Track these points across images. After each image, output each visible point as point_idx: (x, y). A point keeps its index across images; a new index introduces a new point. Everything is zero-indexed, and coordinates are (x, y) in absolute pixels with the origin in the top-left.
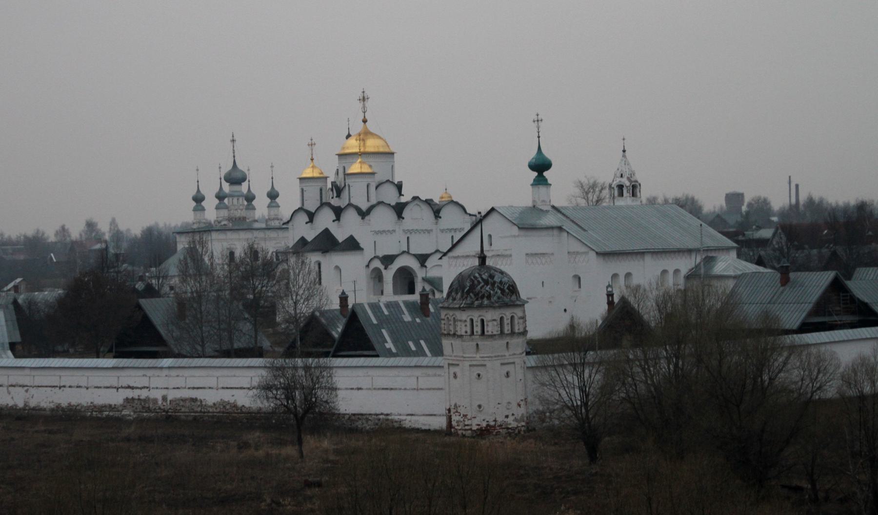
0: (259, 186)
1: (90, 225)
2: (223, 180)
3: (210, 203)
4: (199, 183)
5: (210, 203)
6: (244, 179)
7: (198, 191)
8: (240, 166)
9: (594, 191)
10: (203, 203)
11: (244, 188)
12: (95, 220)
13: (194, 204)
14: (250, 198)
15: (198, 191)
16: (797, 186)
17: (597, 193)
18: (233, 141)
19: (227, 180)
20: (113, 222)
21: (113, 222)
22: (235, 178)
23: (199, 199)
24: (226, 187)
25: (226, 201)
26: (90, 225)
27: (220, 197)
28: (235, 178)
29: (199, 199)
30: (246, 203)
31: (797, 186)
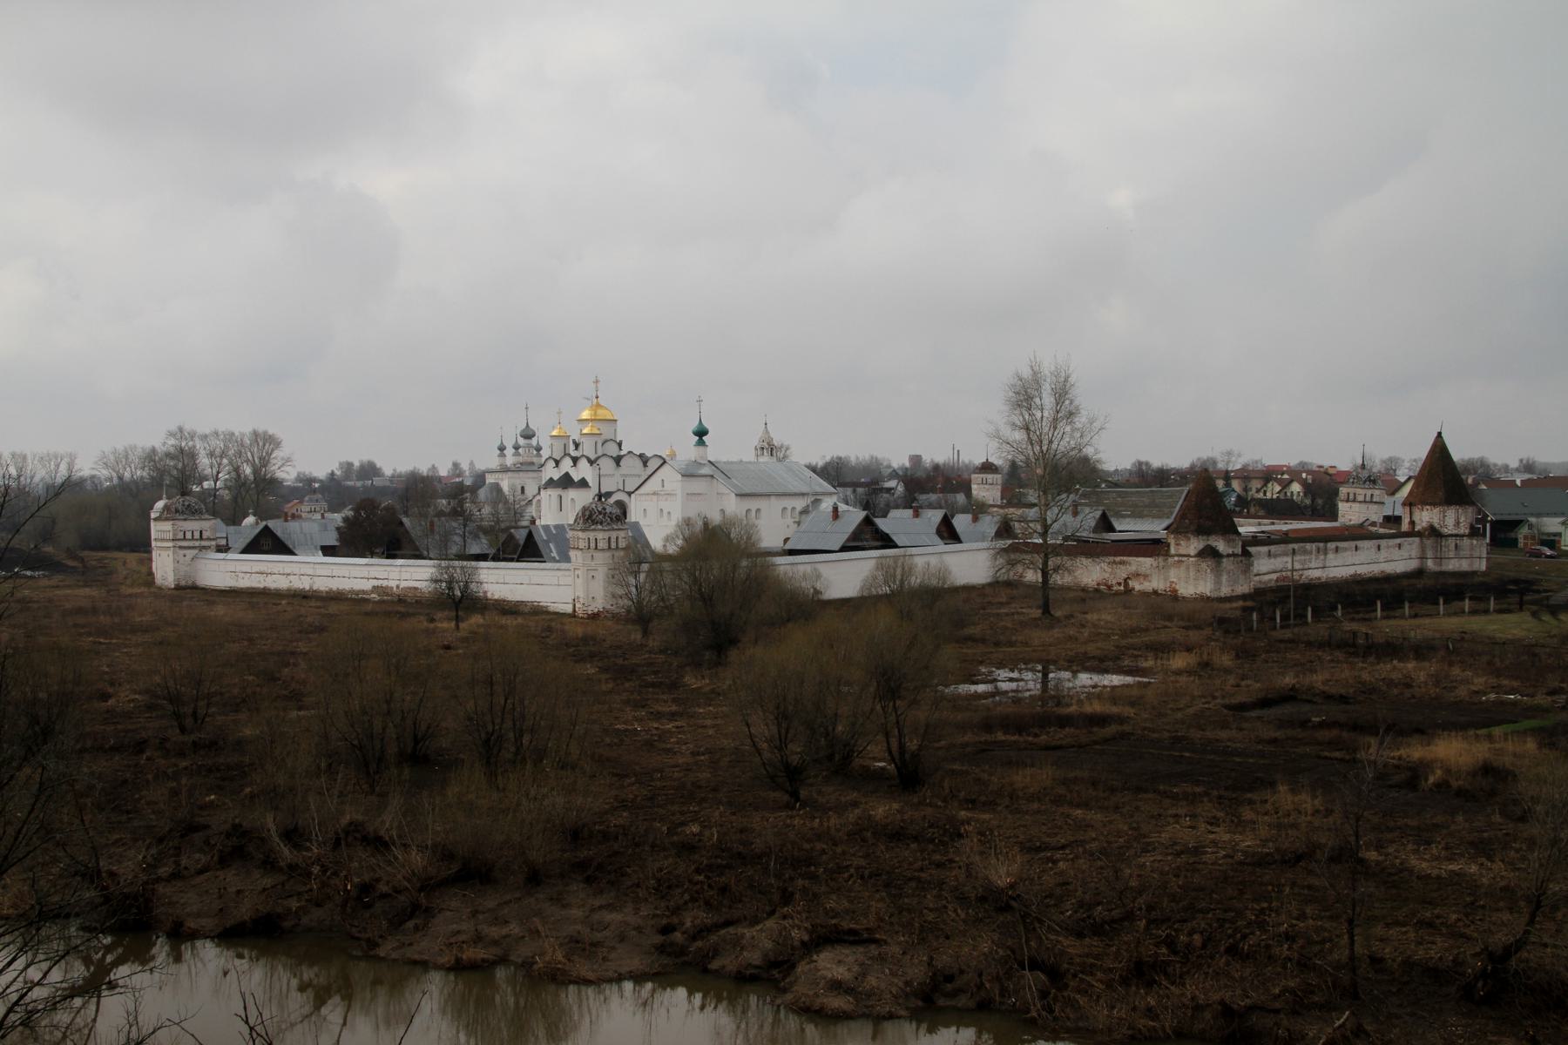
0: (542, 439)
1: (456, 465)
2: (518, 436)
3: (509, 451)
4: (768, 425)
5: (509, 451)
6: (534, 436)
7: (502, 443)
8: (531, 426)
9: (781, 451)
10: (505, 452)
11: (534, 442)
12: (458, 461)
13: (499, 452)
14: (539, 449)
15: (502, 443)
16: (958, 451)
17: (783, 452)
18: (527, 408)
19: (522, 436)
20: (472, 463)
21: (472, 463)
22: (528, 435)
23: (502, 449)
24: (522, 441)
25: (520, 450)
26: (456, 465)
27: (516, 447)
28: (528, 435)
29: (502, 449)
30: (535, 452)
31: (958, 451)
